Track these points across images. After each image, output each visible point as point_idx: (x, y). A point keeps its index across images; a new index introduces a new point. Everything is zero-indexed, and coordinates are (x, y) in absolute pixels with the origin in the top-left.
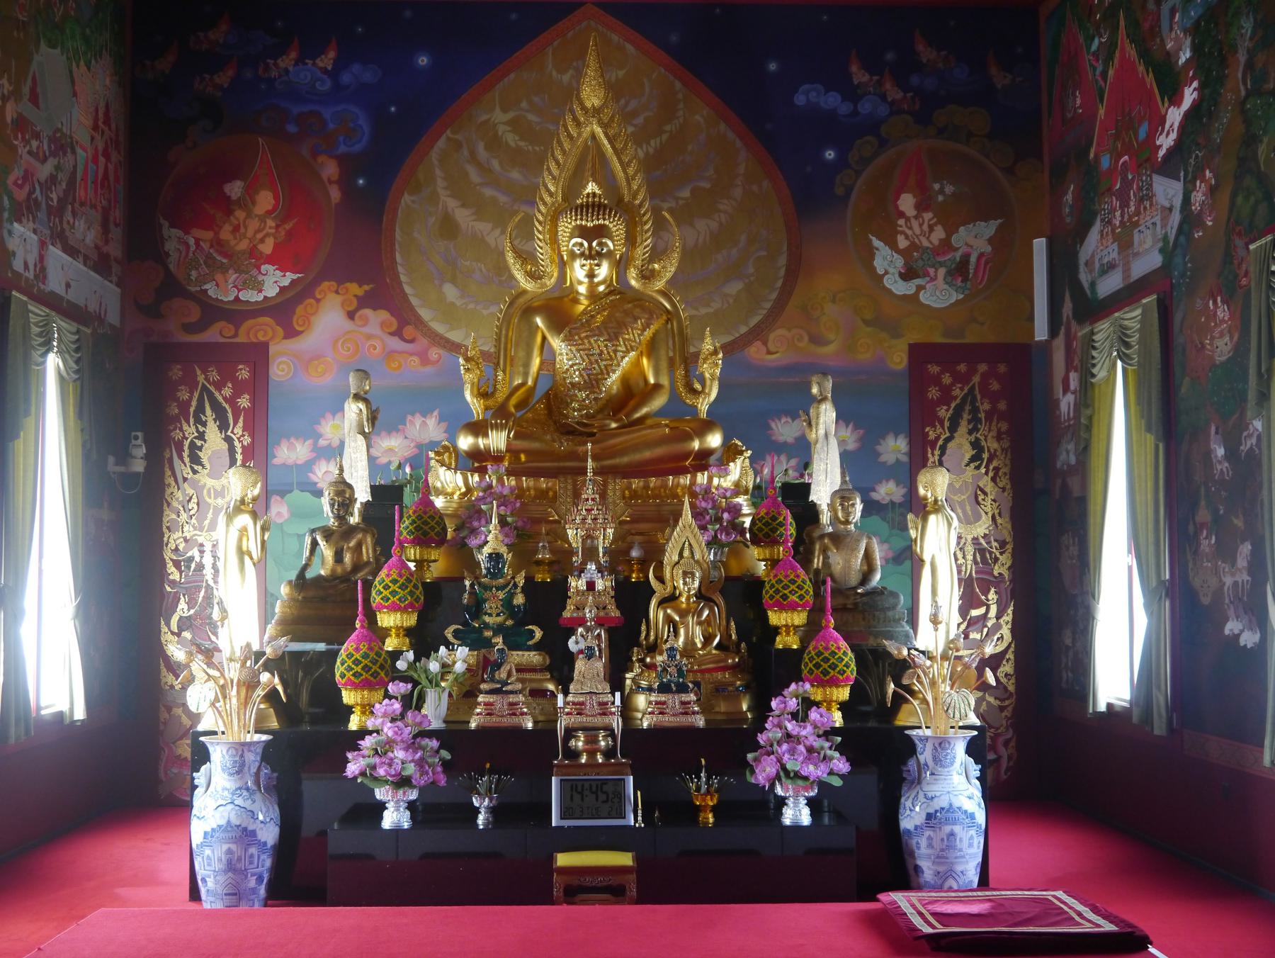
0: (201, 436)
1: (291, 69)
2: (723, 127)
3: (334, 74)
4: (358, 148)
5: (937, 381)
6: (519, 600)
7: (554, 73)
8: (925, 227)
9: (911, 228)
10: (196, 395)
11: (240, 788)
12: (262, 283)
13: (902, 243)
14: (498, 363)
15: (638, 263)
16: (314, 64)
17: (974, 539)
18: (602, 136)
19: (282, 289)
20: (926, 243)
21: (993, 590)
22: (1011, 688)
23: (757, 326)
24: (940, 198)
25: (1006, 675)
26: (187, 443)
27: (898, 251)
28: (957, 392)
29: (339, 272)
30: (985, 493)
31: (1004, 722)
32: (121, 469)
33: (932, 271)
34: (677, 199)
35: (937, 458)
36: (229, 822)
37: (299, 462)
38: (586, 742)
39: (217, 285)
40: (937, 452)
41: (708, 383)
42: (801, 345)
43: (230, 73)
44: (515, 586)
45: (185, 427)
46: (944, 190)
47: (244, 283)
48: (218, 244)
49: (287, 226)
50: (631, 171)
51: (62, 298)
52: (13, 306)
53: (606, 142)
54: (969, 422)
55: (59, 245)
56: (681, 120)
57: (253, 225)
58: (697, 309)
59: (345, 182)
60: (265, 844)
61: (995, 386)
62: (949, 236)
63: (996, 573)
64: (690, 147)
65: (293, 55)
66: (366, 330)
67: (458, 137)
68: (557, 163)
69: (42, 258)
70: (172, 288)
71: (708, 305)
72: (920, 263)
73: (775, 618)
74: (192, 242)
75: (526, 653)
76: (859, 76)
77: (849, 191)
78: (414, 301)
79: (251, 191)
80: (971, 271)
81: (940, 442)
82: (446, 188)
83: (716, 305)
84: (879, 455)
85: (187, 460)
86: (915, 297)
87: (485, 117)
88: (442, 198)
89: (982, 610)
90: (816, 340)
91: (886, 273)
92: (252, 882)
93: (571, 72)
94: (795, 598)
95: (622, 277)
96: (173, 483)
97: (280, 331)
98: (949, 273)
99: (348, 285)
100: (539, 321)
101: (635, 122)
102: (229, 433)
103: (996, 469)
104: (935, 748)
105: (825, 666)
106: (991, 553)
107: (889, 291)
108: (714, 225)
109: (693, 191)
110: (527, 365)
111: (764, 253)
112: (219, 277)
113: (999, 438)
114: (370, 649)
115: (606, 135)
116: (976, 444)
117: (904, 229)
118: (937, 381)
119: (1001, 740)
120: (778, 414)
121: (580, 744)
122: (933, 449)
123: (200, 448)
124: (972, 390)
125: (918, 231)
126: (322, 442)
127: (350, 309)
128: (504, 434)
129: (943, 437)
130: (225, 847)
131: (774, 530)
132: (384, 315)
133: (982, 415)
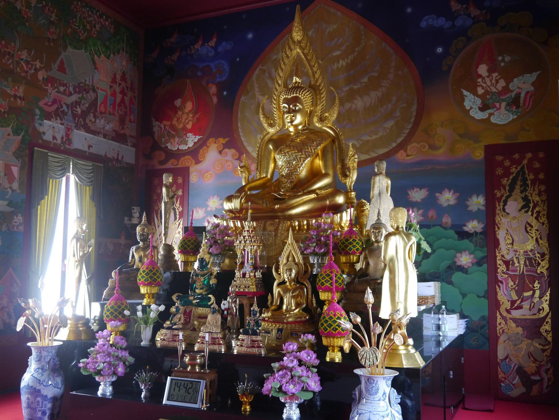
1: (199, 48)
2: (384, 44)
3: (215, 48)
4: (224, 78)
5: (501, 164)
6: (213, 281)
8: (494, 81)
9: (485, 83)
11: (39, 368)
12: (187, 141)
13: (480, 91)
14: (257, 169)
15: (319, 113)
16: (208, 45)
17: (524, 252)
18: (301, 54)
19: (195, 143)
20: (494, 90)
21: (537, 282)
22: (550, 339)
23: (401, 143)
24: (502, 64)
25: (546, 331)
27: (478, 96)
28: (513, 170)
29: (215, 134)
30: (532, 226)
31: (545, 359)
32: (129, 222)
33: (497, 105)
34: (361, 83)
35: (501, 207)
36: (28, 384)
37: (200, 218)
38: (190, 360)
40: (502, 204)
41: (352, 171)
43: (178, 54)
44: (211, 274)
46: (505, 59)
48: (172, 127)
49: (197, 116)
50: (315, 69)
51: (87, 152)
52: (35, 155)
53: (303, 57)
54: (521, 186)
55: (83, 130)
56: (363, 44)
57: (185, 117)
58: (371, 137)
59: (219, 94)
60: (46, 396)
61: (537, 165)
62: (508, 84)
63: (539, 272)
64: (368, 57)
65: (200, 43)
66: (227, 158)
67: (264, 68)
68: (282, 70)
69: (67, 135)
70: (156, 146)
71: (376, 134)
72: (491, 101)
73: (323, 296)
74: (163, 126)
75: (204, 309)
76: (455, 6)
77: (450, 67)
78: (245, 144)
79: (184, 103)
80: (522, 102)
81: (504, 198)
82: (259, 92)
84: (468, 206)
86: (487, 121)
87: (275, 57)
88: (257, 96)
89: (530, 293)
90: (432, 147)
91: (471, 108)
92: (39, 414)
93: (312, 30)
94: (328, 284)
95: (310, 122)
97: (194, 162)
98: (508, 105)
100: (271, 147)
103: (538, 212)
104: (366, 382)
105: (325, 325)
106: (535, 260)
107: (473, 118)
108: (379, 94)
109: (369, 79)
110: (268, 168)
112: (172, 140)
113: (539, 194)
114: (116, 304)
115: (303, 53)
116: (526, 199)
117: (482, 83)
118: (501, 164)
119: (543, 369)
120: (413, 187)
121: (187, 360)
122: (499, 202)
124: (523, 168)
125: (489, 83)
126: (209, 209)
128: (239, 200)
129: (505, 195)
130: (27, 396)
132: (233, 151)
133: (529, 182)
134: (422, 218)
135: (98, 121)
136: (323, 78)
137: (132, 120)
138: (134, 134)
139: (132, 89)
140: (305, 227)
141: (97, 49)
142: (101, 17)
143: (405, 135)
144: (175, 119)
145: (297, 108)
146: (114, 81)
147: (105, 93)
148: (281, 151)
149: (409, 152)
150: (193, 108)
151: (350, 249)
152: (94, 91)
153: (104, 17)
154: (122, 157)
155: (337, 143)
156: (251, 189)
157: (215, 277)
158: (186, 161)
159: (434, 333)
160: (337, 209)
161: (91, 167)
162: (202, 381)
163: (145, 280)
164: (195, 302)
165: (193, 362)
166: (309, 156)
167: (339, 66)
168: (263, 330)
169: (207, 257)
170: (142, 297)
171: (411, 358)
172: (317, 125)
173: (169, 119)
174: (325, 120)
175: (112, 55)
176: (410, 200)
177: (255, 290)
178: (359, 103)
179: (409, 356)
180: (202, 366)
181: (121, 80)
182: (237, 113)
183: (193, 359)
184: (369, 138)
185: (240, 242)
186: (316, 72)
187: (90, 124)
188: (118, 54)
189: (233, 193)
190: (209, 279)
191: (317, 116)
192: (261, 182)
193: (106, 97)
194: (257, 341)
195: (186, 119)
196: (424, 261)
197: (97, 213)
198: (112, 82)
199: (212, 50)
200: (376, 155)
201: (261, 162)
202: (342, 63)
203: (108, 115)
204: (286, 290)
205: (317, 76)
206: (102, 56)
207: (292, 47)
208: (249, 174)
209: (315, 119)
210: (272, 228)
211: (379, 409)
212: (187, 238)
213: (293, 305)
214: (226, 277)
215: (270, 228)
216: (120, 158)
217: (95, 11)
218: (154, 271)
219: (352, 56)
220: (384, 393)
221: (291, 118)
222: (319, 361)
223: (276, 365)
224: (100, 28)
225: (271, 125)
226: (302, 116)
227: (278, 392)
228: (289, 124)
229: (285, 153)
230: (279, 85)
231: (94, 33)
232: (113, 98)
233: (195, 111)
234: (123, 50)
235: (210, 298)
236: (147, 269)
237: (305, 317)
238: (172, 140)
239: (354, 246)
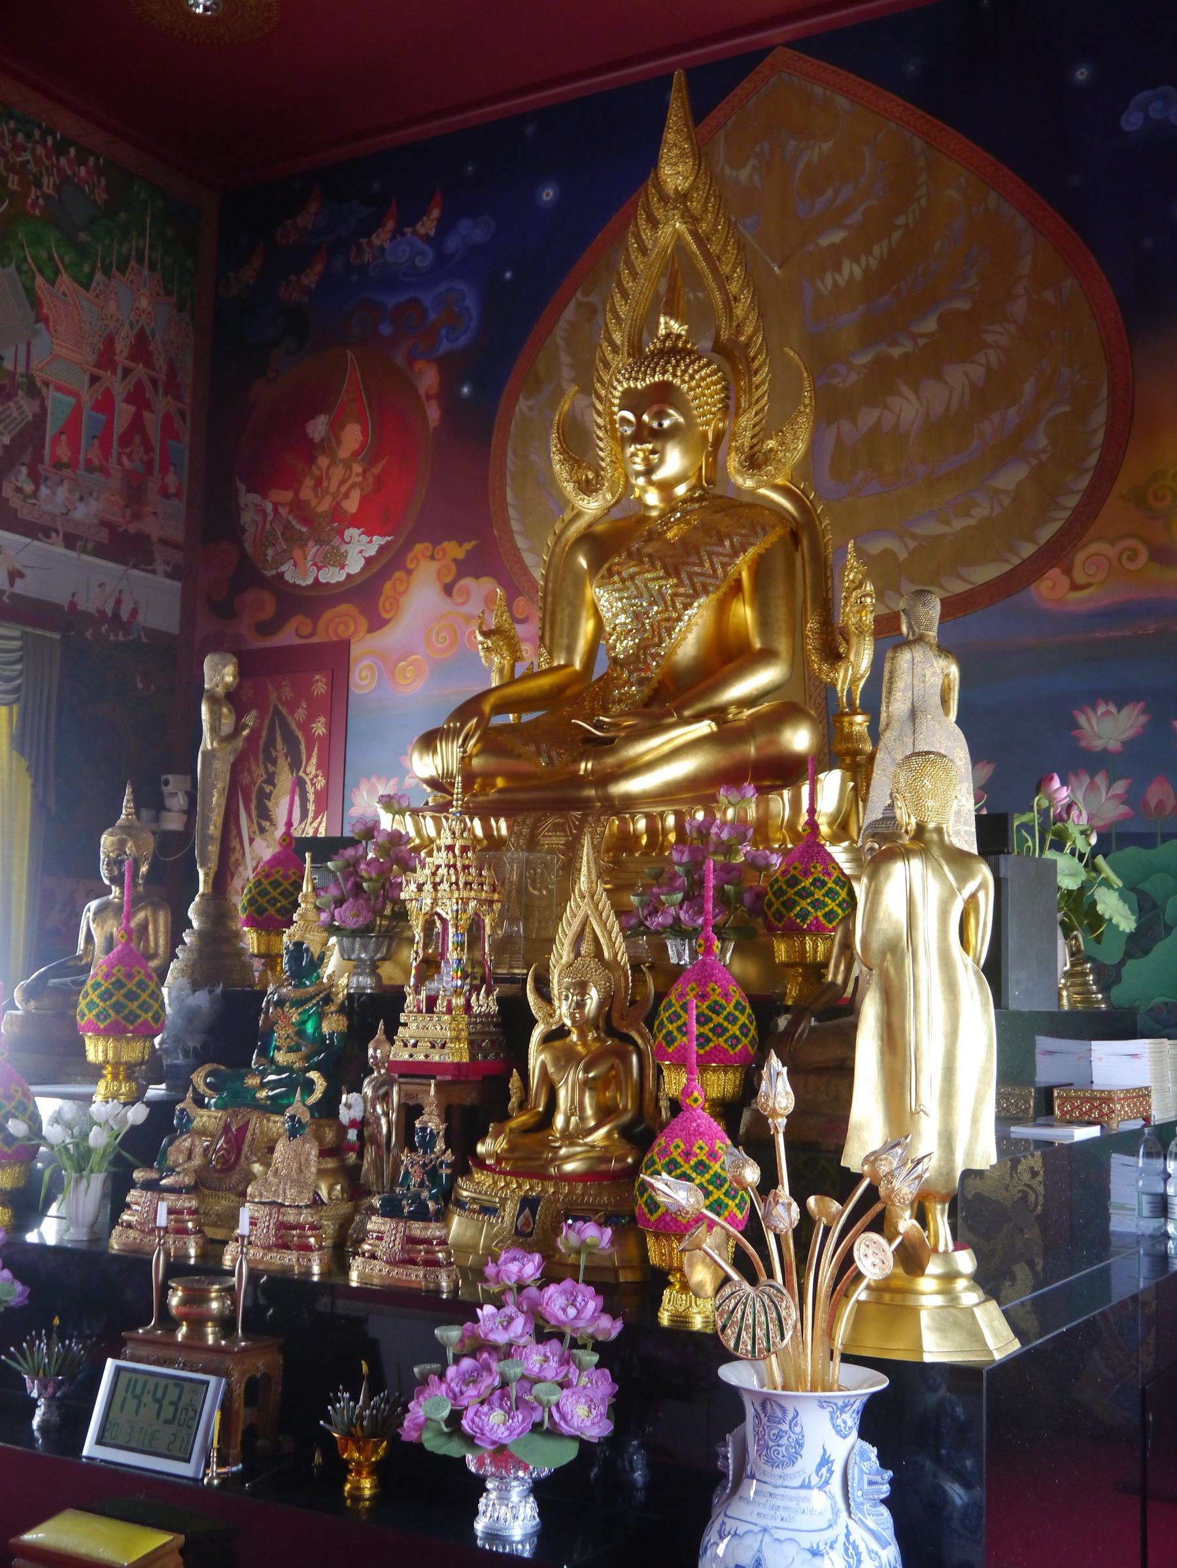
0: (271, 780)
1: (387, 245)
2: (993, 198)
3: (437, 241)
4: (463, 341)
6: (333, 1025)
7: (727, 171)
10: (267, 721)
12: (344, 556)
14: (542, 638)
15: (745, 440)
16: (415, 233)
18: (689, 238)
19: (369, 561)
23: (1053, 541)
26: (255, 789)
29: (433, 530)
34: (914, 337)
38: (184, 1302)
39: (295, 565)
41: (854, 640)
42: (1132, 567)
43: (319, 267)
44: (328, 1000)
45: (254, 768)
47: (325, 558)
48: (299, 508)
50: (733, 288)
53: (694, 247)
56: (923, 202)
57: (338, 473)
58: (947, 523)
59: (446, 394)
64: (937, 246)
65: (390, 225)
67: (592, 298)
70: (248, 574)
71: (967, 514)
74: (269, 508)
79: (336, 428)
82: (573, 380)
83: (979, 513)
85: (254, 813)
93: (752, 162)
96: (238, 847)
97: (364, 623)
99: (445, 544)
101: (849, 221)
102: (301, 774)
104: (757, 1416)
108: (977, 372)
111: (1066, 408)
120: (1091, 699)
123: (268, 796)
127: (448, 580)
131: (790, 904)
132: (487, 585)
134: (1123, 809)
135: (44, 491)
136: (761, 316)
137: (172, 490)
138: (177, 533)
139: (172, 388)
140: (672, 837)
141: (44, 254)
142: (60, 149)
143: (1066, 514)
144: (309, 482)
145: (666, 423)
146: (106, 359)
147: (73, 400)
148: (610, 573)
149: (1079, 577)
150: (363, 445)
151: (804, 915)
152: (33, 391)
153: (72, 151)
154: (134, 613)
155: (805, 543)
156: (502, 707)
157: (341, 1010)
158: (339, 621)
159: (1149, 1226)
160: (788, 772)
161: (18, 643)
162: (212, 1379)
163: (97, 1016)
164: (263, 1094)
165: (195, 1310)
166: (706, 592)
167: (842, 282)
168: (474, 1200)
169: (313, 942)
170: (94, 1073)
171: (961, 1323)
172: (739, 480)
173: (291, 482)
174: (766, 462)
175: (98, 276)
176: (1083, 743)
177: (466, 1059)
178: (908, 408)
179: (958, 1320)
180: (226, 1324)
181: (132, 357)
182: (504, 455)
183: (195, 1298)
184: (941, 529)
185: (420, 888)
186: (736, 299)
187: (15, 502)
188: (122, 269)
189: (439, 722)
190: (321, 1016)
191: (737, 449)
192: (545, 682)
193: (77, 410)
194: (427, 1241)
195: (343, 482)
196: (1131, 963)
197: (35, 795)
198: (98, 365)
199: (426, 247)
200: (968, 587)
201: (553, 614)
202: (851, 270)
203: (81, 472)
204: (567, 1059)
205: (739, 311)
206: (65, 277)
207: (659, 214)
208: (516, 657)
209: (733, 462)
210: (558, 841)
211: (802, 1522)
212: (267, 876)
213: (589, 1112)
214: (378, 1010)
215: (553, 840)
216: (125, 615)
217: (37, 133)
218: (131, 985)
219: (885, 243)
220: (825, 1461)
221: (646, 460)
222: (619, 1326)
223: (450, 1334)
224: (57, 188)
225: (587, 488)
226: (686, 451)
227: (450, 1435)
228: (641, 481)
229: (623, 581)
230: (615, 350)
231: (35, 204)
232: (103, 417)
233: (371, 454)
234: (140, 259)
235: (311, 1082)
236: (107, 976)
237: (624, 1159)
238: (297, 553)
239: (817, 904)
